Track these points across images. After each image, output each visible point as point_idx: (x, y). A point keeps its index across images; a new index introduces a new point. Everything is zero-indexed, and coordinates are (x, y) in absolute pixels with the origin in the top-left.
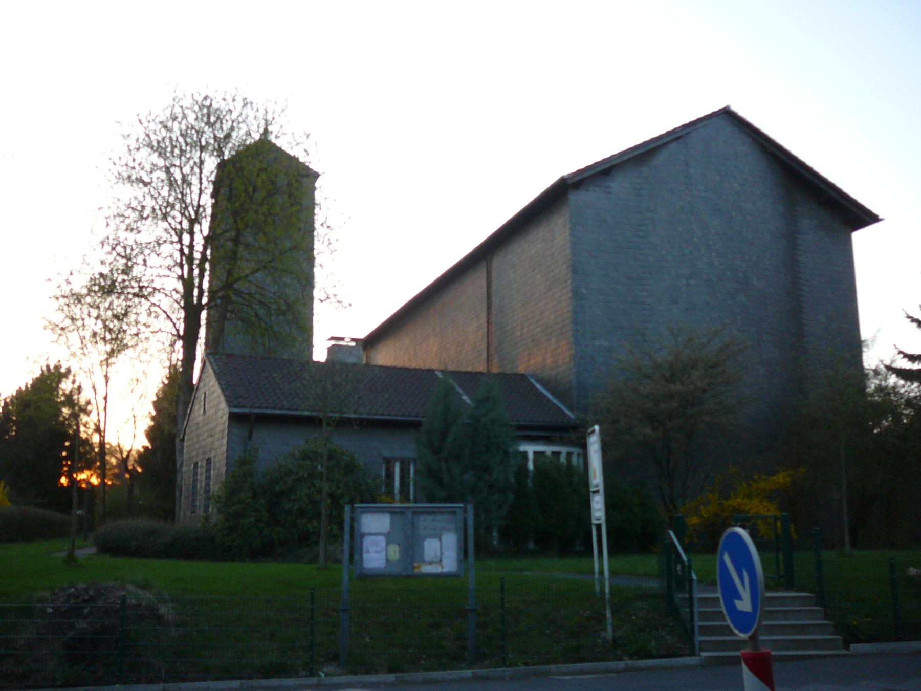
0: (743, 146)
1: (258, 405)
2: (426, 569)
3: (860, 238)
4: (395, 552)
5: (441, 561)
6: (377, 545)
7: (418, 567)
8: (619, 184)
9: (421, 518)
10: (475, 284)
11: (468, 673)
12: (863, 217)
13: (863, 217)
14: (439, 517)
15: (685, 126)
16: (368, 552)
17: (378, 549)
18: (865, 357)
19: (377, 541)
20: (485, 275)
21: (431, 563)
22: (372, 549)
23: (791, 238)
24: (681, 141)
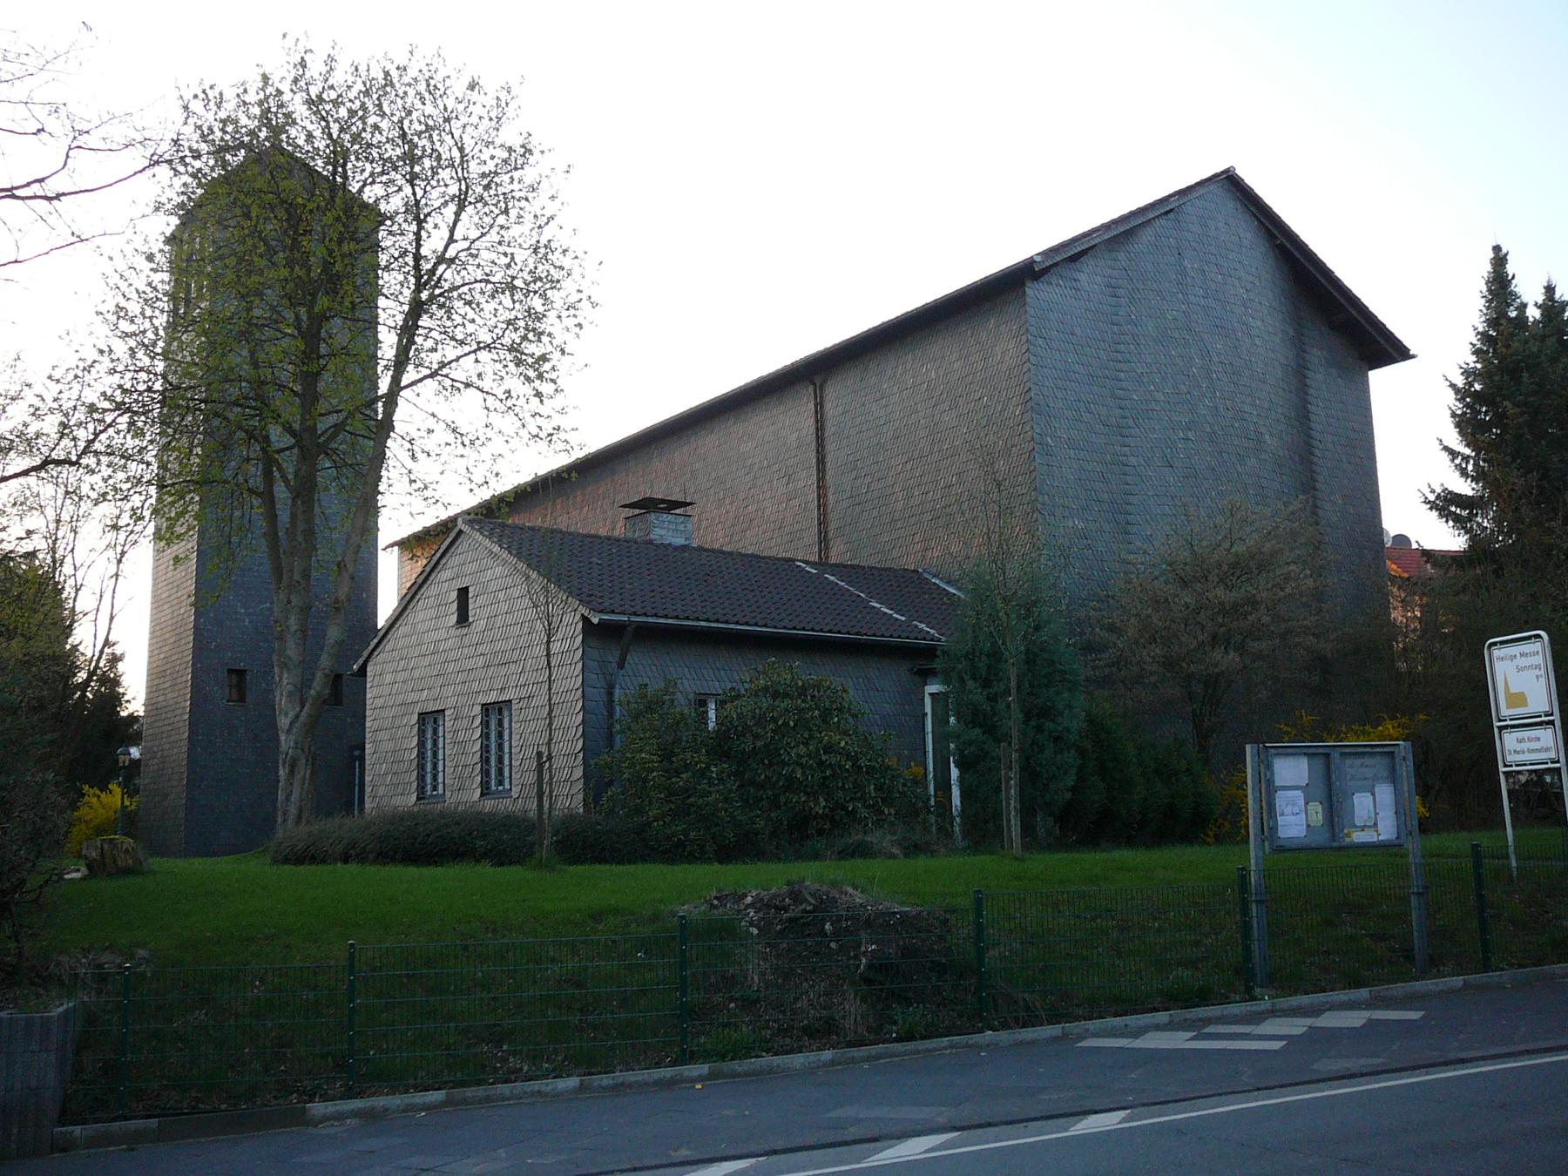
0: (1247, 232)
1: (641, 611)
2: (1359, 837)
3: (1381, 381)
4: (1317, 813)
5: (1376, 824)
6: (1294, 805)
7: (1348, 835)
8: (1089, 276)
9: (1348, 762)
10: (792, 421)
11: (1458, 981)
12: (1388, 349)
13: (1388, 349)
14: (1368, 761)
15: (1181, 193)
16: (1282, 814)
17: (1296, 810)
18: (1456, 548)
19: (1290, 796)
20: (812, 406)
21: (1363, 828)
22: (1288, 810)
23: (1299, 373)
24: (1171, 215)
